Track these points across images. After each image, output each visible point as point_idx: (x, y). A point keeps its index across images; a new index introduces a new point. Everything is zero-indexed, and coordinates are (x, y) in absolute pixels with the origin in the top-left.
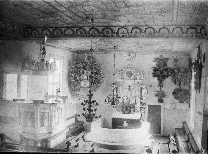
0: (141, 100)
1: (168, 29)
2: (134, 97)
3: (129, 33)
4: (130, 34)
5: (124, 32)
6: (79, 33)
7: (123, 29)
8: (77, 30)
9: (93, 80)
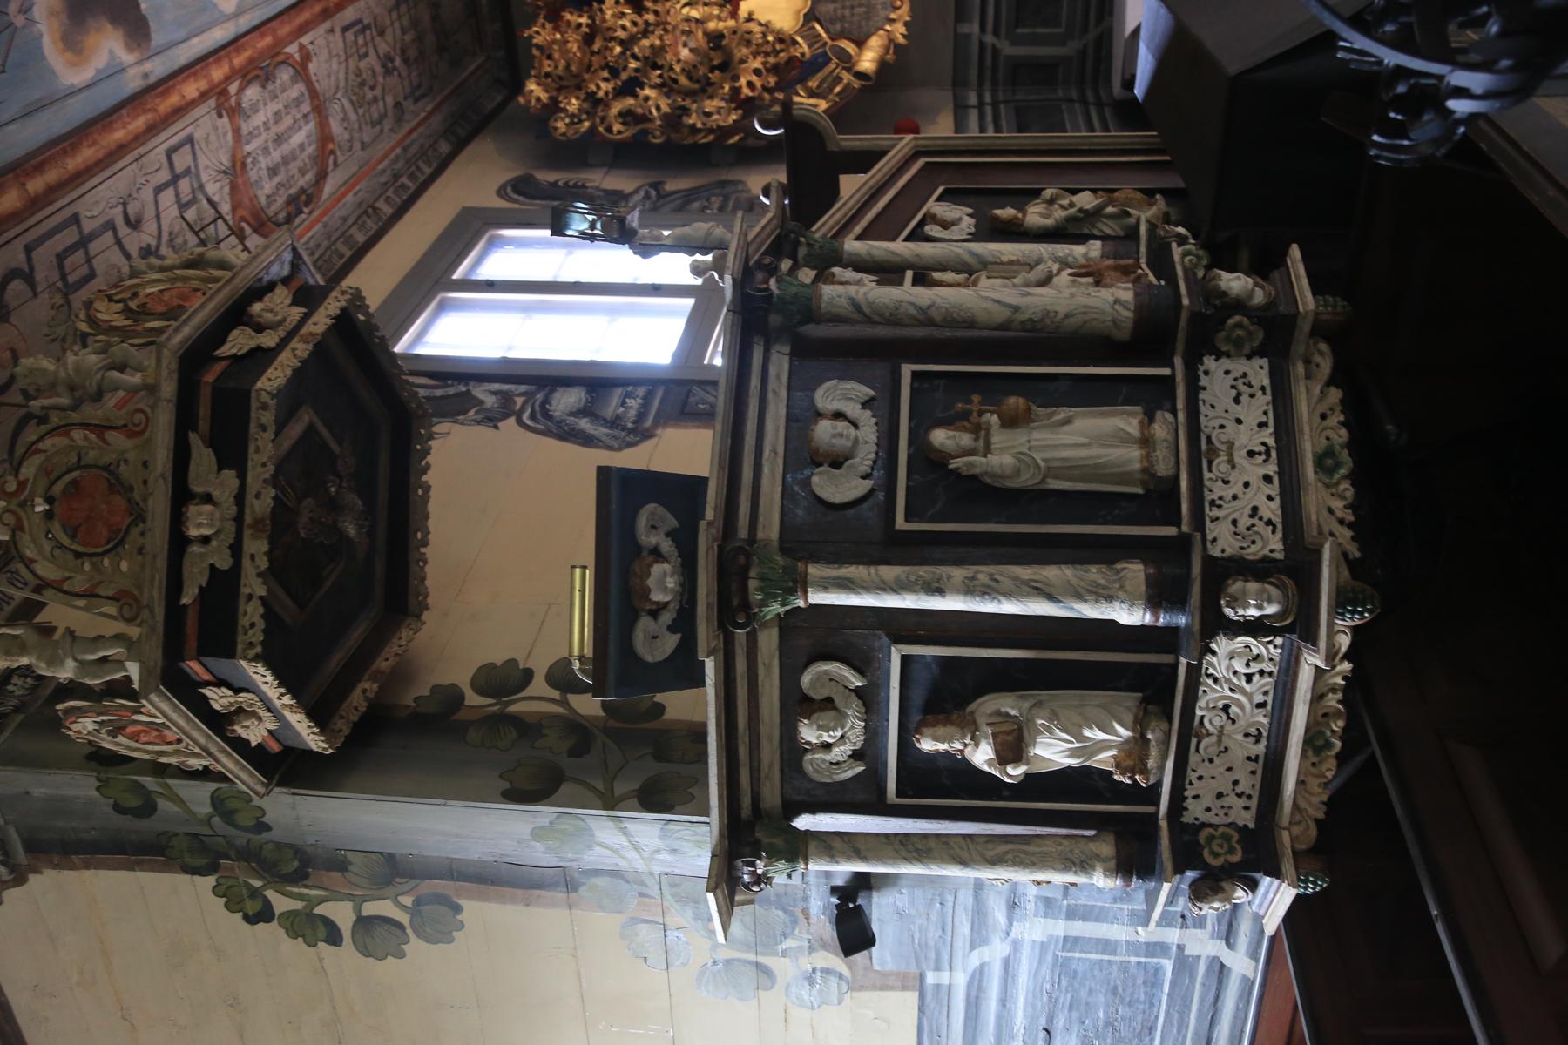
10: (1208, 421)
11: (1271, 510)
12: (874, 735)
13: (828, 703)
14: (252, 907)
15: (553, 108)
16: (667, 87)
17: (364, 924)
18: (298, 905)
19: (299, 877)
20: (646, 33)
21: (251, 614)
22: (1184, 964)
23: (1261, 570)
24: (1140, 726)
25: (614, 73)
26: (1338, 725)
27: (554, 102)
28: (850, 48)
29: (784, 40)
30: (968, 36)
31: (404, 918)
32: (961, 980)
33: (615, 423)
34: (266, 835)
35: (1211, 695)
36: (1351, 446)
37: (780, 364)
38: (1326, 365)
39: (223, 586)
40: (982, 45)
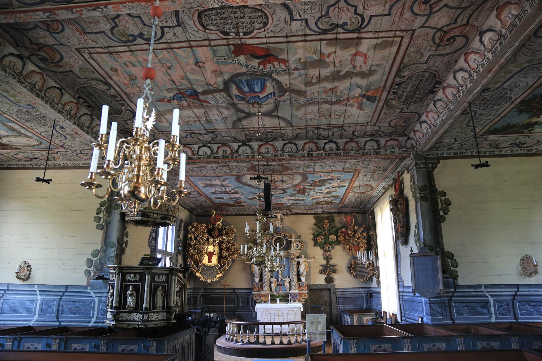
0: (299, 282)
1: (357, 143)
2: (288, 277)
3: (299, 151)
4: (301, 152)
5: (291, 150)
6: (221, 152)
7: (291, 144)
8: (219, 147)
9: (224, 253)
10: (161, 313)
11: (153, 319)
12: (132, 282)
13: (135, 277)
14: (102, 204)
15: (193, 227)
16: (195, 244)
17: (100, 218)
18: (103, 210)
19: (107, 211)
20: (203, 241)
21: (145, 219)
22: (91, 318)
23: (148, 318)
24: (133, 307)
25: (198, 236)
26: (131, 327)
27: (194, 227)
28: (200, 271)
29: (201, 262)
30: (201, 290)
31: (100, 223)
32: (88, 291)
33: (151, 242)
34: (113, 209)
35: (135, 315)
36: (158, 327)
37: (167, 272)
38: (165, 324)
39: (149, 217)
40: (199, 292)
